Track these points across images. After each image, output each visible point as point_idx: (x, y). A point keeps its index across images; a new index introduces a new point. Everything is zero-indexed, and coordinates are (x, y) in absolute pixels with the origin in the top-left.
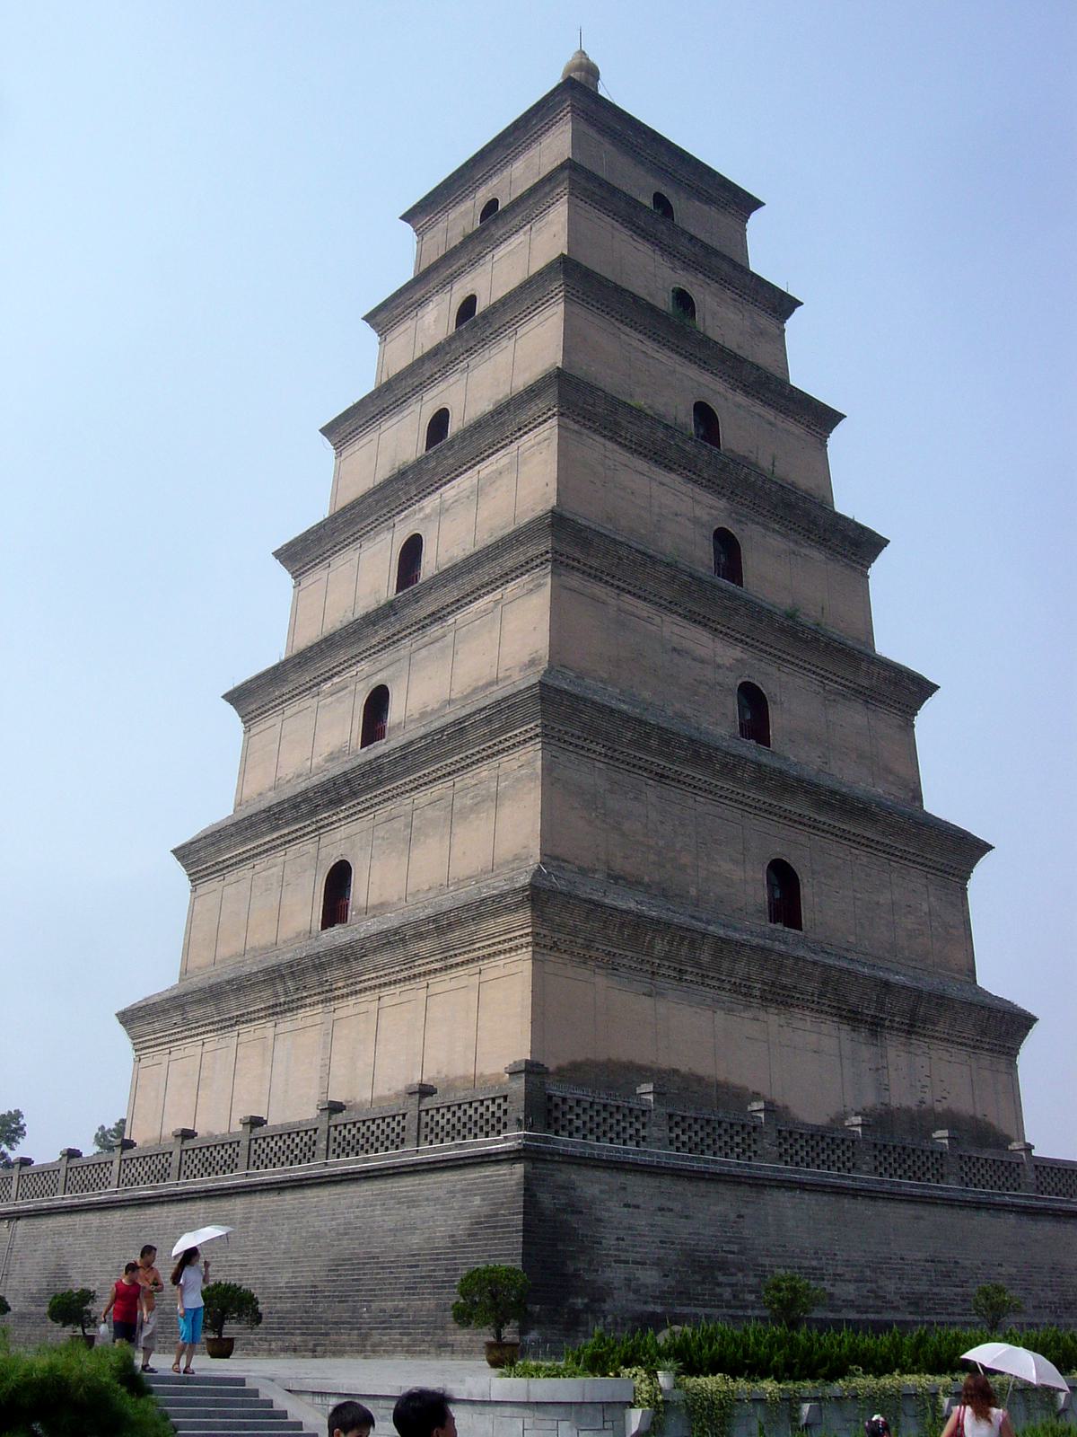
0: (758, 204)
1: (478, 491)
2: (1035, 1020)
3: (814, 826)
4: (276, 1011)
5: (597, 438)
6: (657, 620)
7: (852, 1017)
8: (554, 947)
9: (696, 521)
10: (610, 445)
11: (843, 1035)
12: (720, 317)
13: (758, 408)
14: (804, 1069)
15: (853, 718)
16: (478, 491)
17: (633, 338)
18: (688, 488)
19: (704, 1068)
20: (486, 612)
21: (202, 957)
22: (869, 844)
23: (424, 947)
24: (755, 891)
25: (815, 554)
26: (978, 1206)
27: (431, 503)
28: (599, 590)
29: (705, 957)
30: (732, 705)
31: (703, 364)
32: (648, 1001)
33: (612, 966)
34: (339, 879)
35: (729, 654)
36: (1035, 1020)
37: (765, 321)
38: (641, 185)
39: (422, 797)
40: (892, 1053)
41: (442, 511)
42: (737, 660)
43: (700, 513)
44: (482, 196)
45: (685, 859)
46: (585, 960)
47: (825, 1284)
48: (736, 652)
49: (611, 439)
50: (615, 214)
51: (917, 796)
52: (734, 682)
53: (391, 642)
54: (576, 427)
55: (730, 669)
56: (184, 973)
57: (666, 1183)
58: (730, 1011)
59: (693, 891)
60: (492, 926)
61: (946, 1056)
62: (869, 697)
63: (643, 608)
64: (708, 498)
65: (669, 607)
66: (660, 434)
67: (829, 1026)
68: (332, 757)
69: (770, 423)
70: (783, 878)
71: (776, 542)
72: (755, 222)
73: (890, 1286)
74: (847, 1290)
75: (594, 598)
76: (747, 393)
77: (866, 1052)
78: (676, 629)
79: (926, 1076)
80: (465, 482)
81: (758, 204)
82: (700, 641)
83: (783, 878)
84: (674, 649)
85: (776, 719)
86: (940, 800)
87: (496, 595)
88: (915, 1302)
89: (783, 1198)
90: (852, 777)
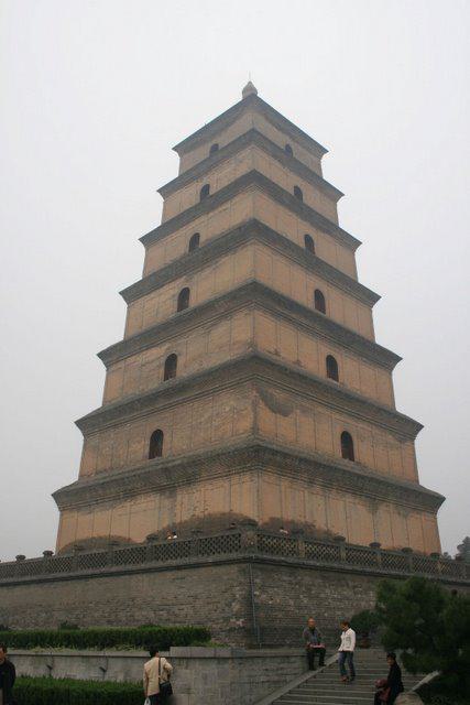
3: (171, 406)
7: (161, 490)
9: (174, 296)
13: (220, 209)
17: (169, 238)
22: (197, 397)
33: (78, 509)
40: (179, 498)
43: (172, 292)
48: (167, 345)
52: (163, 360)
61: (210, 487)
63: (132, 359)
64: (178, 281)
65: (141, 351)
77: (167, 502)
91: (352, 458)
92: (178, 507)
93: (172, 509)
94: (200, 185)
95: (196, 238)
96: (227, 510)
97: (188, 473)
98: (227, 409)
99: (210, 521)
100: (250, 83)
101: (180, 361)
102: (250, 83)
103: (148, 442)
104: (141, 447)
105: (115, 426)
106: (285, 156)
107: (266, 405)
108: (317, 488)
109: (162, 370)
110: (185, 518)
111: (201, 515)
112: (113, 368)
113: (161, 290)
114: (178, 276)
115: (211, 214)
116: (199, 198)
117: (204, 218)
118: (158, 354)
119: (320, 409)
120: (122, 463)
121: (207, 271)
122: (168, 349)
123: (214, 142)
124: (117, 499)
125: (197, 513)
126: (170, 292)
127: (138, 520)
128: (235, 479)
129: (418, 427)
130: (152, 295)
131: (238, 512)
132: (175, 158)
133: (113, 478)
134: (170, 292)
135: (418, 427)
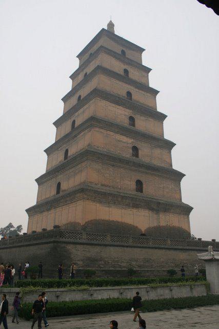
0: (144, 50)
1: (84, 112)
2: (191, 209)
3: (146, 173)
4: (48, 210)
7: (152, 209)
11: (150, 213)
12: (134, 74)
13: (141, 91)
14: (142, 220)
15: (157, 152)
16: (84, 112)
17: (114, 80)
18: (124, 109)
19: (120, 220)
20: (83, 135)
21: (44, 197)
23: (68, 199)
24: (132, 185)
26: (156, 248)
27: (77, 114)
29: (120, 199)
30: (131, 151)
31: (129, 84)
32: (107, 208)
33: (100, 202)
34: (59, 185)
35: (130, 141)
36: (191, 209)
37: (144, 74)
38: (118, 49)
39: (71, 171)
40: (161, 216)
41: (78, 115)
43: (127, 114)
44: (89, 52)
45: (118, 181)
46: (94, 201)
47: (120, 264)
48: (132, 140)
50: (112, 55)
51: (172, 166)
52: (131, 146)
53: (69, 141)
56: (37, 202)
57: (85, 246)
59: (119, 187)
60: (78, 195)
62: (161, 147)
63: (112, 133)
66: (117, 99)
67: (147, 211)
68: (60, 162)
70: (139, 184)
71: (143, 118)
72: (144, 54)
73: (134, 263)
74: (124, 264)
75: (101, 132)
76: (139, 89)
79: (169, 220)
80: (82, 110)
81: (144, 50)
82: (124, 139)
83: (139, 184)
85: (140, 152)
86: (176, 166)
87: (84, 132)
88: (140, 266)
89: (112, 248)
90: (157, 163)
99: (174, 228)
100: (111, 21)
102: (111, 21)
105: (113, 166)
110: (164, 225)
113: (118, 107)
114: (128, 108)
115: (137, 90)
118: (128, 141)
120: (119, 187)
124: (128, 205)
128: (182, 216)
130: (114, 105)
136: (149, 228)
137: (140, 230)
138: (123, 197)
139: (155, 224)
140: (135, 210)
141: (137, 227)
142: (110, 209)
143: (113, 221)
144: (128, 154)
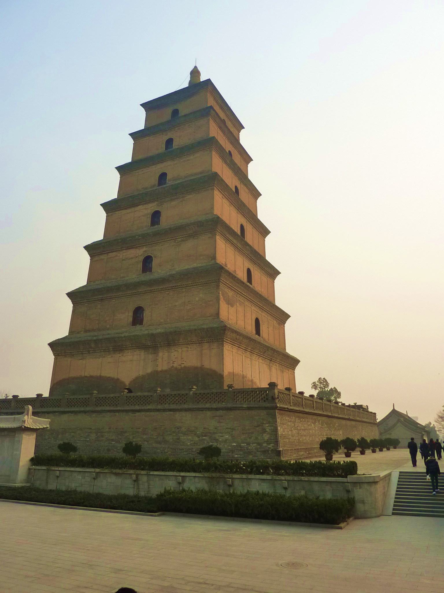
5: (117, 212)
6: (119, 255)
8: (58, 355)
10: (120, 212)
15: (188, 246)
25: (190, 196)
28: (102, 257)
29: (93, 345)
32: (81, 361)
40: (161, 354)
42: (144, 252)
46: (65, 356)
48: (145, 249)
49: (121, 210)
52: (142, 258)
54: (111, 214)
55: (141, 256)
58: (104, 357)
63: (114, 254)
64: (150, 205)
69: (188, 160)
77: (151, 356)
78: (124, 254)
82: (132, 253)
84: (124, 260)
91: (259, 335)
92: (160, 360)
93: (156, 360)
94: (166, 138)
95: (163, 176)
96: (199, 365)
97: (169, 340)
98: (197, 299)
100: (196, 67)
101: (155, 263)
102: (196, 67)
103: (131, 314)
104: (127, 316)
105: (102, 300)
106: (222, 125)
107: (224, 299)
108: (248, 353)
109: (140, 265)
111: (179, 367)
112: (96, 258)
113: (137, 208)
116: (164, 146)
117: (169, 163)
119: (247, 303)
120: (108, 326)
121: (173, 203)
122: (145, 251)
123: (176, 107)
125: (175, 365)
126: (144, 212)
127: (128, 367)
129: (287, 316)
130: (128, 211)
131: (208, 367)
132: (142, 113)
133: (105, 337)
134: (144, 212)
135: (287, 316)
136: (137, 378)
137: (122, 383)
138: (96, 341)
139: (149, 371)
140: (117, 356)
141: (118, 379)
142: (84, 362)
143: (86, 377)
144: (134, 275)
